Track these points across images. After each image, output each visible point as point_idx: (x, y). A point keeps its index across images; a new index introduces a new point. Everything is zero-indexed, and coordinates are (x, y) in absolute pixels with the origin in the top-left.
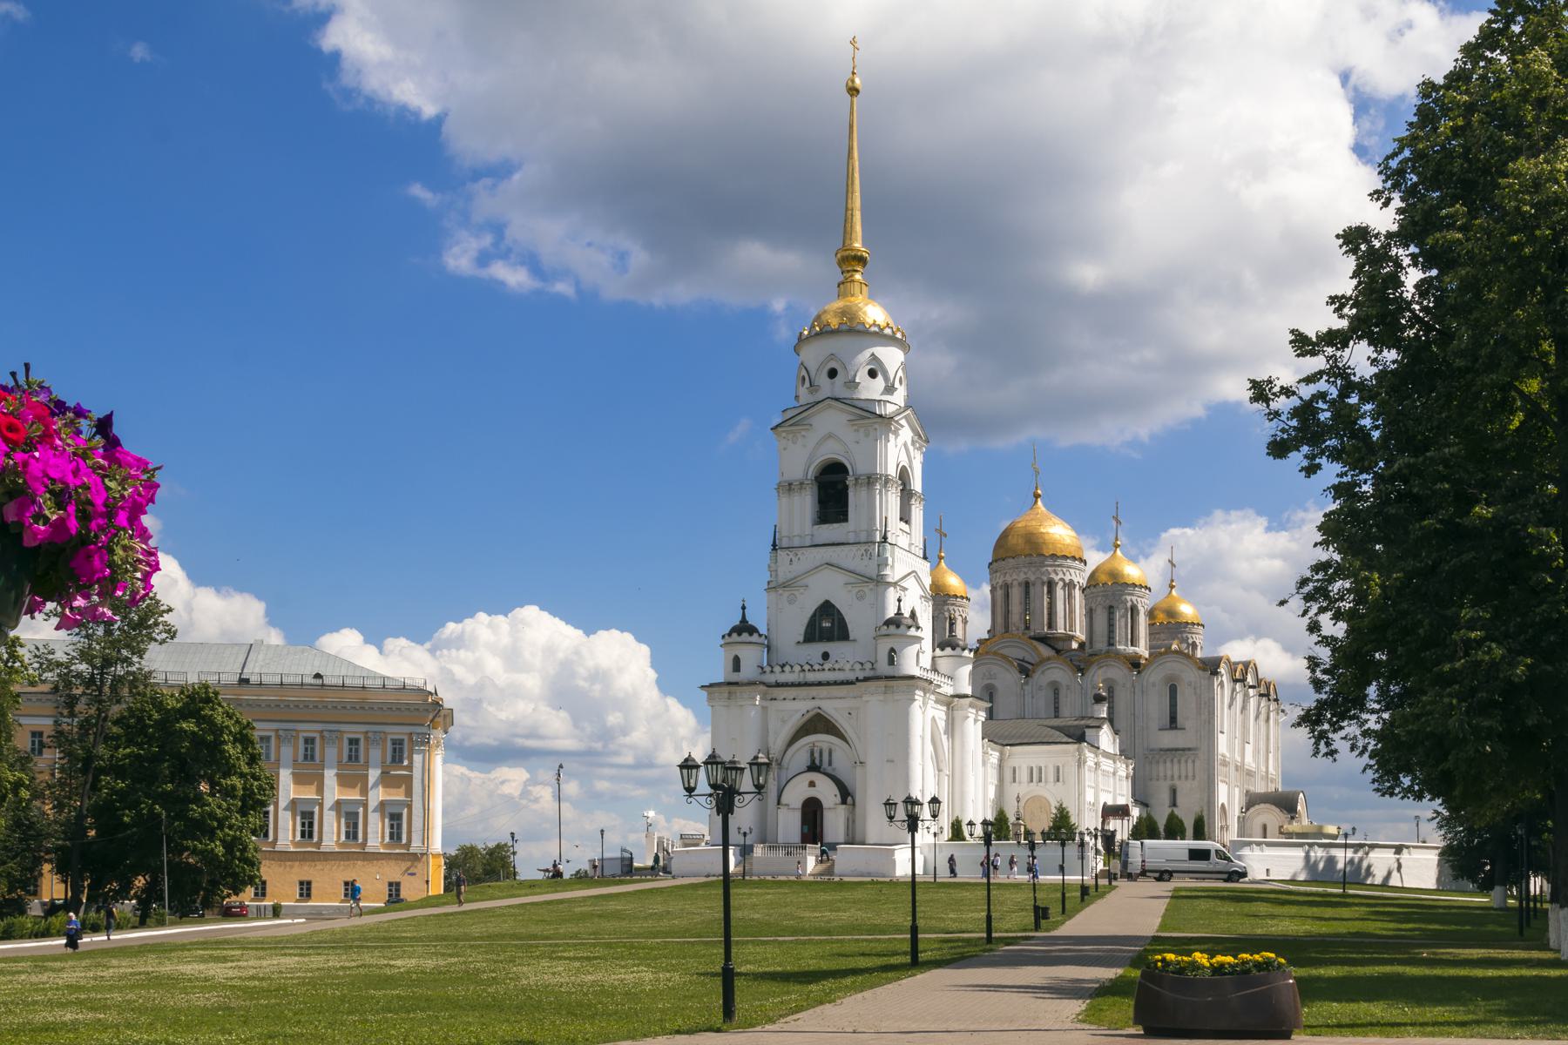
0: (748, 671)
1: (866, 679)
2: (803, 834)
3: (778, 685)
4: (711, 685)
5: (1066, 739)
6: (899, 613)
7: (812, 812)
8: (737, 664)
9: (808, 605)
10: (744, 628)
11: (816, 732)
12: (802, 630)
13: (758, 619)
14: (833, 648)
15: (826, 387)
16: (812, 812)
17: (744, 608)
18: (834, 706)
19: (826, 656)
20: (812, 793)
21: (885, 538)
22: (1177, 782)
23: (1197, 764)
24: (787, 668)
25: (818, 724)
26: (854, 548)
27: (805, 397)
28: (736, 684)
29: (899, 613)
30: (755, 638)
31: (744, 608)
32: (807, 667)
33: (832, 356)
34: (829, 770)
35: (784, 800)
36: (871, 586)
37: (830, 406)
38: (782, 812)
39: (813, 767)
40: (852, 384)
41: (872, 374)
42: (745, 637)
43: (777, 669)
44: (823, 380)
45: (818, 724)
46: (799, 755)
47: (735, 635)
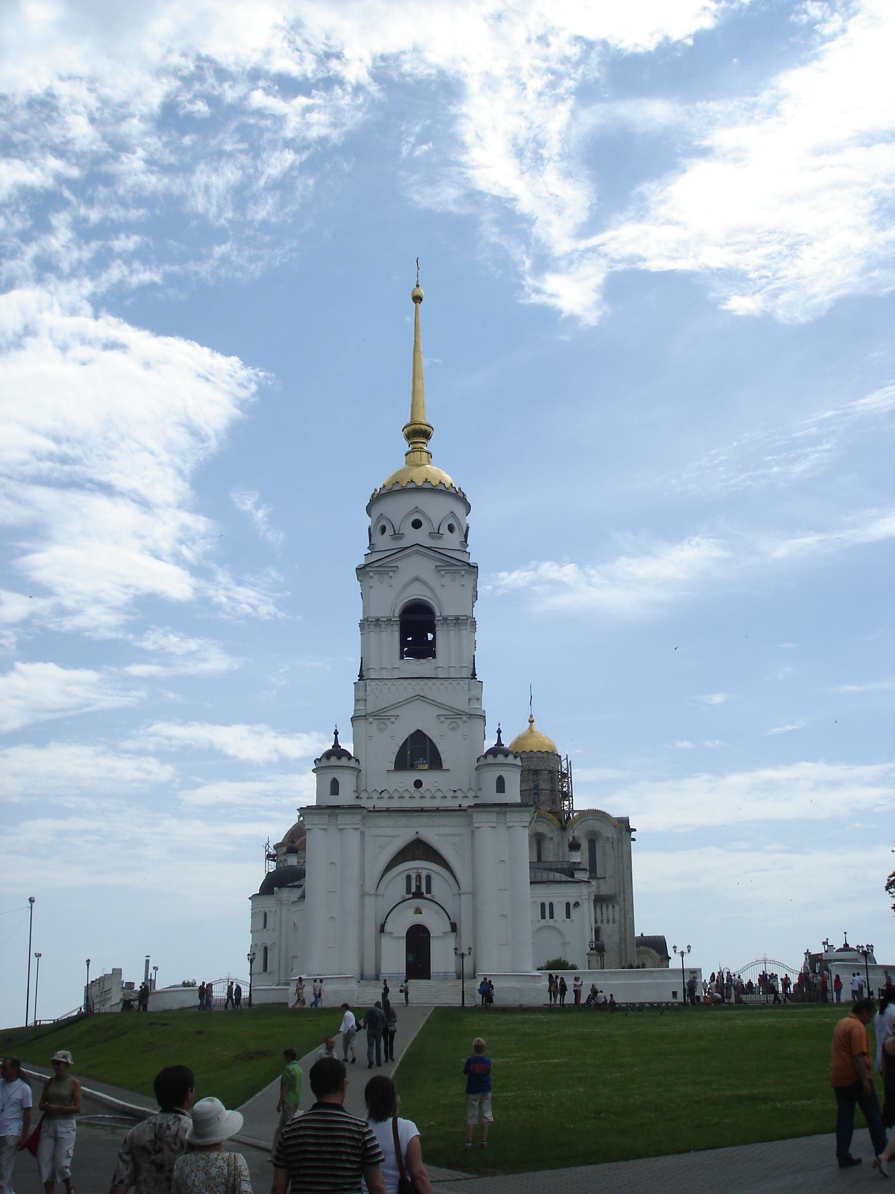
0: (346, 797)
1: (477, 806)
3: (375, 811)
4: (309, 808)
5: (564, 878)
6: (499, 743)
7: (418, 941)
8: (335, 787)
9: (400, 733)
10: (337, 752)
11: (414, 859)
12: (393, 758)
13: (348, 746)
15: (413, 536)
16: (418, 941)
19: (418, 784)
21: (474, 675)
22: (599, 924)
23: (617, 908)
24: (384, 794)
25: (418, 849)
26: (446, 682)
27: (385, 542)
28: (338, 807)
29: (499, 743)
30: (352, 763)
32: (407, 795)
33: (417, 510)
34: (428, 896)
35: (387, 928)
36: (465, 718)
37: (417, 552)
38: (385, 940)
39: (418, 895)
40: (436, 535)
41: (451, 528)
42: (344, 761)
43: (375, 795)
44: (408, 529)
45: (418, 849)
46: (396, 887)
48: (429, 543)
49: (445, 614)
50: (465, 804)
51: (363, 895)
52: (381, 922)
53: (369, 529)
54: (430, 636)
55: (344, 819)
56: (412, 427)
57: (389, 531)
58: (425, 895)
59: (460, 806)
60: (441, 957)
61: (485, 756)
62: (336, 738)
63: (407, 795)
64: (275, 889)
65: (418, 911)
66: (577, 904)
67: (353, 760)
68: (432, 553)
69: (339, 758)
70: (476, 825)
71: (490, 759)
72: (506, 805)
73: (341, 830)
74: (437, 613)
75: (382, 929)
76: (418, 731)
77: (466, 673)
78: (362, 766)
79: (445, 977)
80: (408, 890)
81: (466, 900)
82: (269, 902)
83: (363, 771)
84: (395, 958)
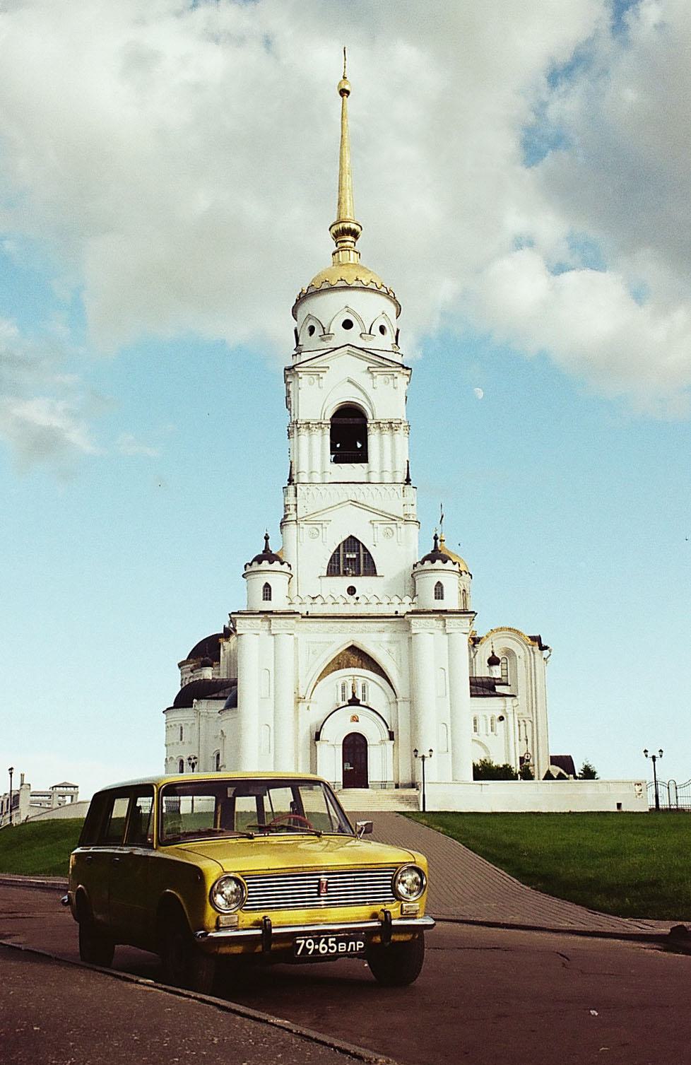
1: (413, 612)
2: (345, 773)
7: (355, 748)
14: (360, 583)
16: (355, 748)
17: (267, 538)
18: (375, 641)
19: (352, 590)
20: (354, 728)
24: (319, 600)
31: (267, 538)
39: (354, 702)
41: (382, 330)
44: (337, 327)
47: (255, 564)
48: (361, 344)
49: (378, 417)
50: (402, 611)
51: (299, 700)
52: (315, 730)
53: (296, 331)
54: (359, 445)
55: (278, 623)
56: (341, 226)
57: (318, 331)
58: (361, 703)
59: (397, 612)
60: (380, 764)
61: (422, 563)
62: (267, 542)
63: (341, 601)
64: (195, 701)
65: (355, 719)
66: (501, 718)
67: (286, 564)
68: (361, 353)
69: (271, 563)
70: (414, 632)
71: (428, 564)
72: (445, 612)
73: (274, 635)
74: (370, 416)
75: (318, 737)
76: (352, 540)
77: (401, 478)
78: (293, 572)
79: (383, 785)
80: (343, 699)
81: (403, 708)
82: (184, 714)
83: (295, 576)
84: (331, 768)
